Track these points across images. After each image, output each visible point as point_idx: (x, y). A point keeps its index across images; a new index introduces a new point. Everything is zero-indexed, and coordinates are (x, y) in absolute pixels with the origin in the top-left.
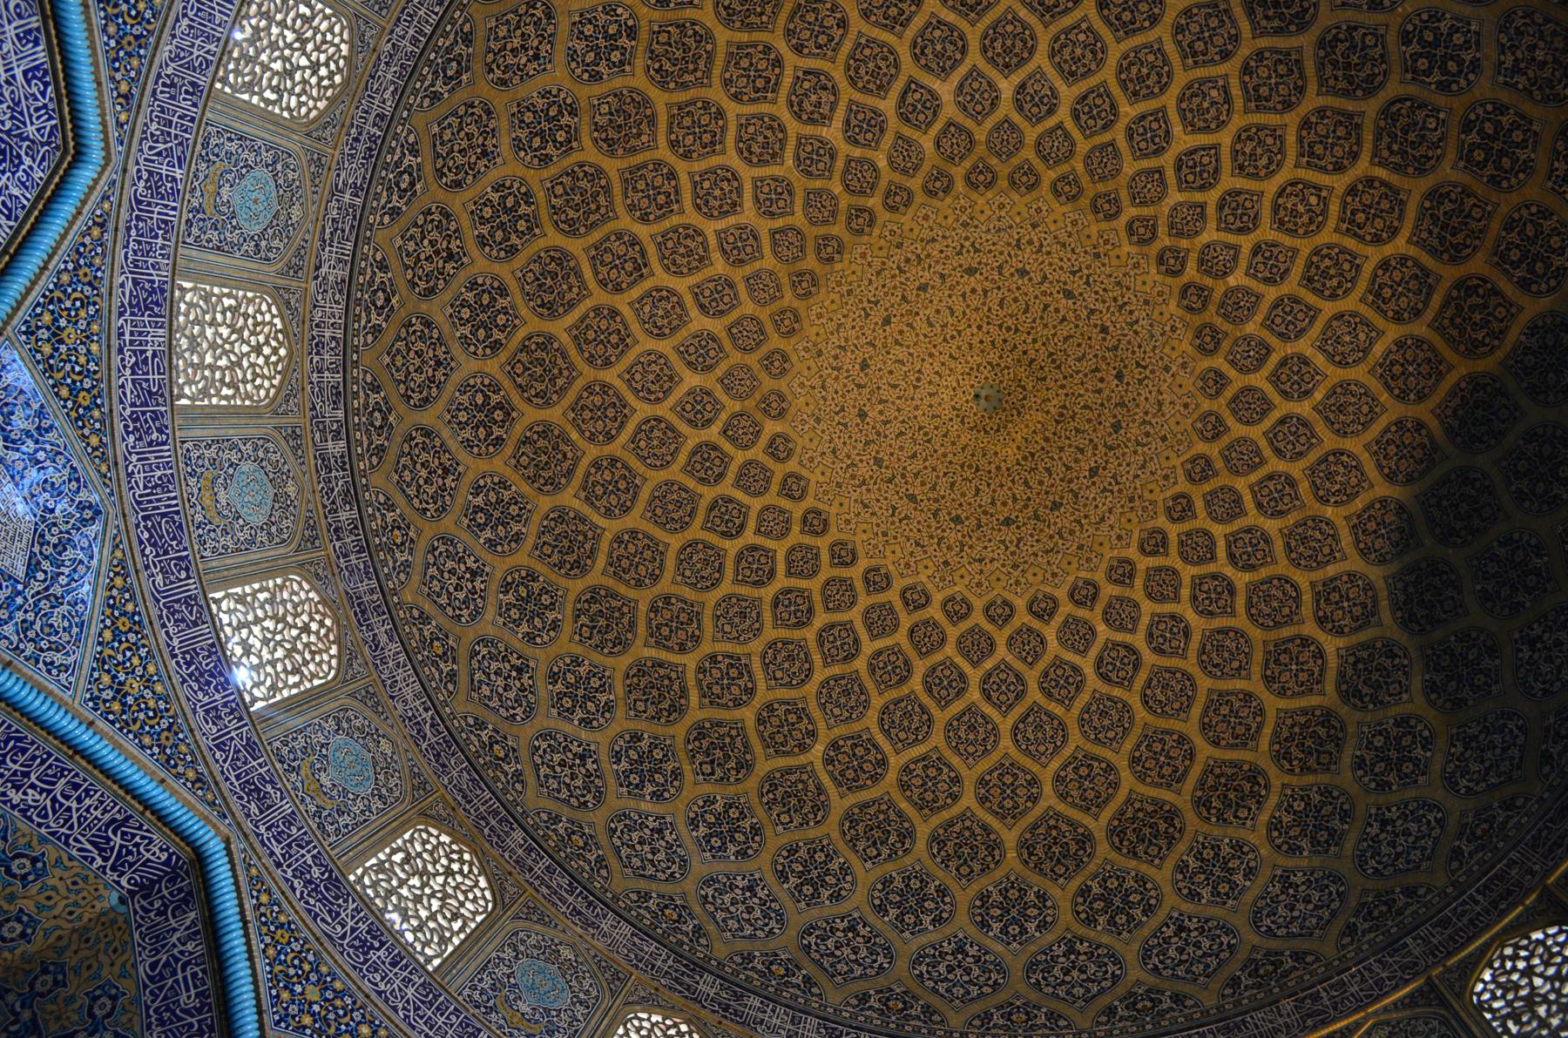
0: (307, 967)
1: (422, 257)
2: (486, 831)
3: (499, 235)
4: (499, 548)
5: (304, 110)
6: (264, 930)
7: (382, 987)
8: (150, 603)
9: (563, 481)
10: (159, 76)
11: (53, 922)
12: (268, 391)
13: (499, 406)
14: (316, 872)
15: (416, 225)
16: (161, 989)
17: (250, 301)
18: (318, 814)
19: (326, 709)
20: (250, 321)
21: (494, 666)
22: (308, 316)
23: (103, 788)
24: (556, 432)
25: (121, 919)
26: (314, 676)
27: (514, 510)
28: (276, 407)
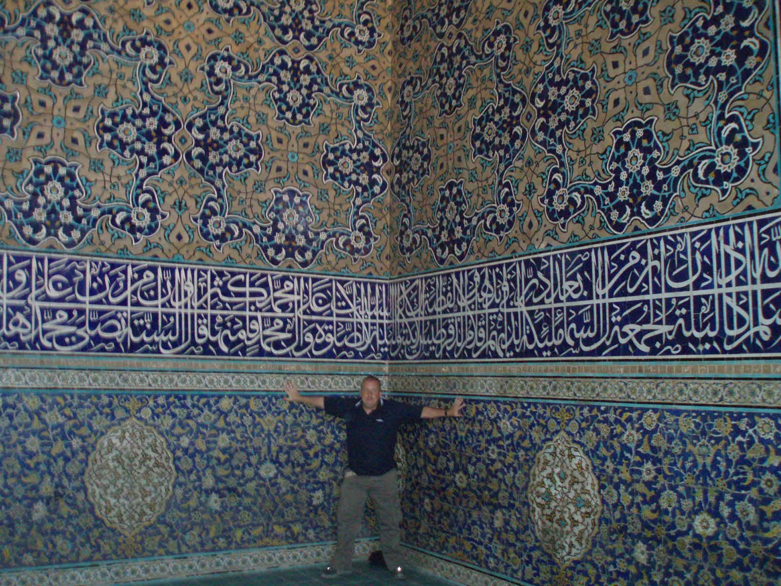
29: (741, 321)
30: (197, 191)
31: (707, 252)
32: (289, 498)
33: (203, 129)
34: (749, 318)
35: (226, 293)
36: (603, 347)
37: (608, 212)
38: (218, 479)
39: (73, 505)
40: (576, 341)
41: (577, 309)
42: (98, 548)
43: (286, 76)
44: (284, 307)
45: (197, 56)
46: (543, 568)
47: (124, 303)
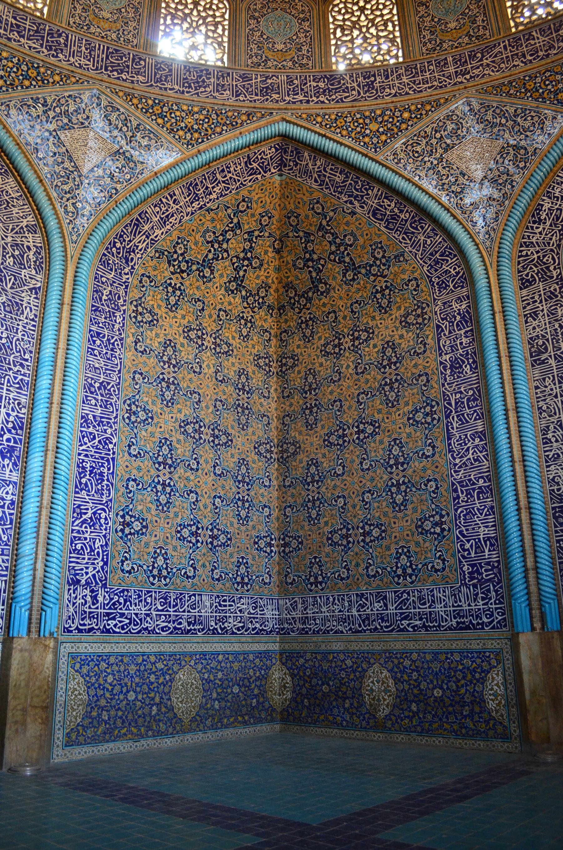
0: (361, 121)
6: (333, 129)
7: (393, 92)
11: (272, 205)
14: (321, 85)
16: (327, 184)
18: (294, 63)
19: (243, 20)
23: (229, 160)
25: (288, 180)
26: (223, 16)
29: (446, 620)
30: (210, 559)
31: (433, 596)
32: (244, 702)
33: (212, 530)
34: (449, 619)
35: (220, 605)
36: (394, 629)
37: (393, 578)
38: (218, 694)
39: (166, 707)
40: (382, 627)
41: (381, 614)
42: (174, 728)
43: (240, 503)
44: (240, 611)
45: (209, 497)
46: (371, 721)
47: (184, 611)
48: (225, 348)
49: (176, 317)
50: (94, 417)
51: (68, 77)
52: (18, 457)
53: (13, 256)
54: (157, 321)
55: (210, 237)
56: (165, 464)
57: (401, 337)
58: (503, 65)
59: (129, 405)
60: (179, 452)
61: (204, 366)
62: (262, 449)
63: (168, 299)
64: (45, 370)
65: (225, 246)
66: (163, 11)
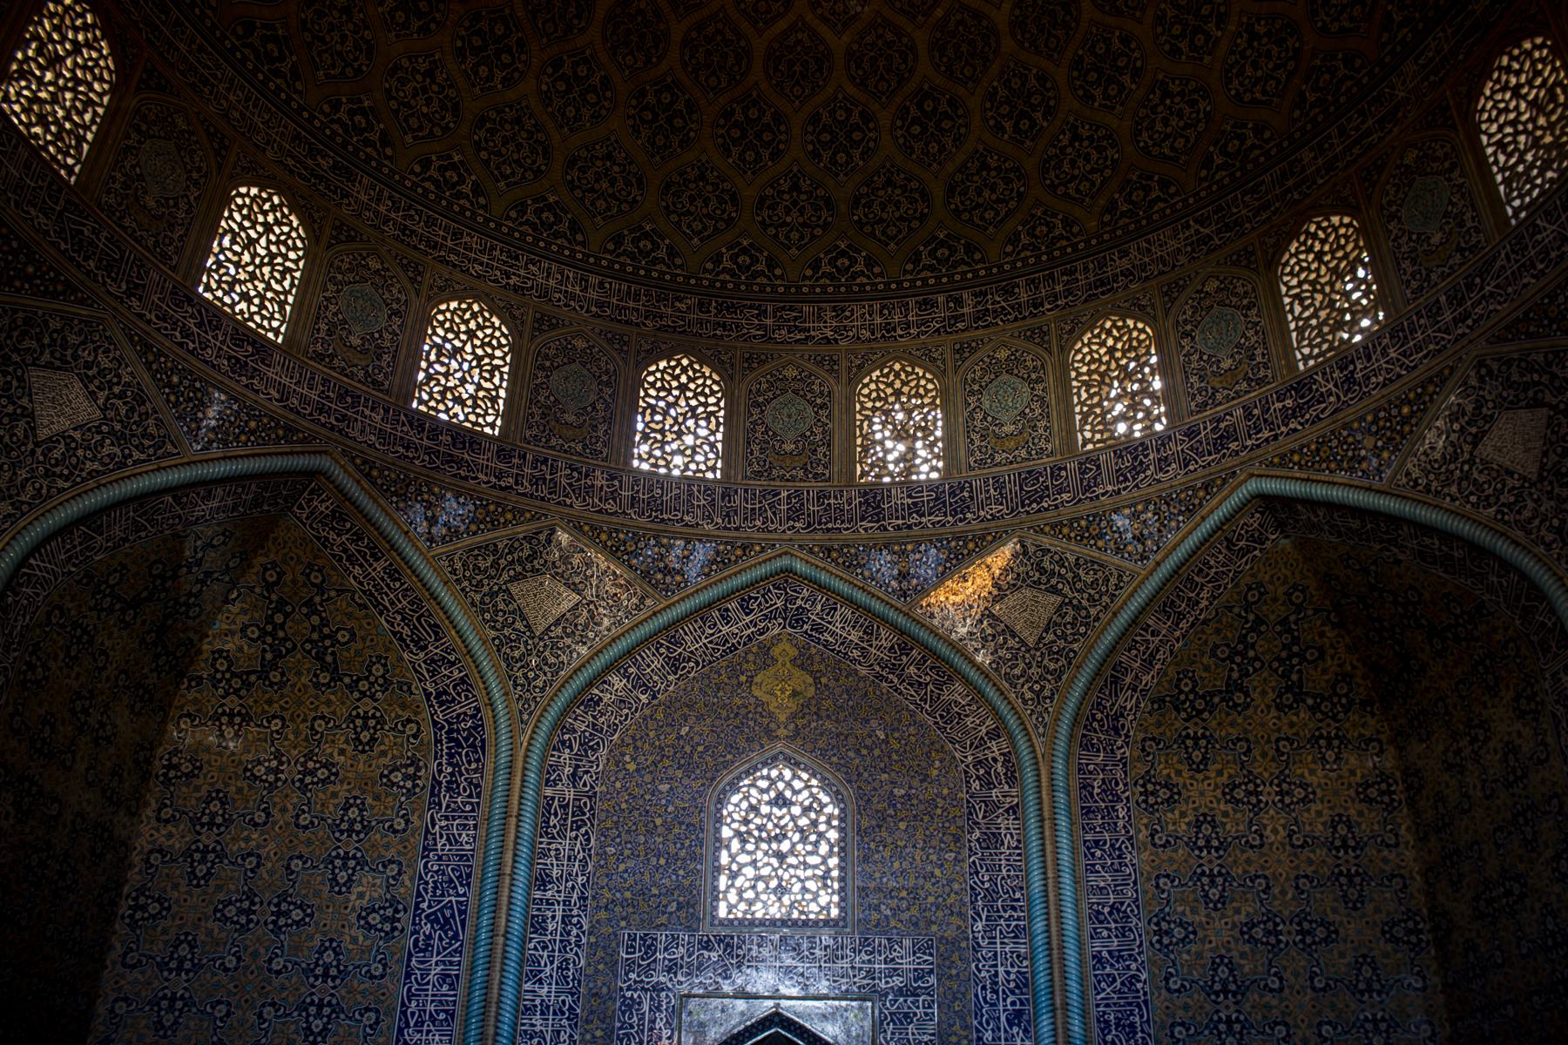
0: (1350, 440)
1: (801, 220)
2: (1296, 197)
3: (767, 137)
4: (1052, 103)
5: (715, 388)
8: (1081, 507)
9: (985, 23)
10: (725, 528)
12: (929, 381)
13: (920, 106)
14: (1289, 403)
15: (776, 236)
17: (863, 408)
20: (878, 404)
21: (1159, 127)
22: (867, 345)
24: (938, 35)
26: (1148, 353)
27: (1016, 83)
28: (941, 374)
43: (1369, 1026)
48: (1299, 793)
49: (1208, 778)
50: (1110, 952)
51: (983, 538)
52: (1028, 1022)
53: (978, 778)
54: (1179, 793)
55: (1223, 652)
56: (1225, 991)
57: (1519, 734)
58: (1510, 290)
59: (1157, 924)
60: (1246, 969)
61: (1267, 832)
62: (1399, 932)
63: (1190, 758)
64: (1038, 909)
65: (1251, 654)
66: (1075, 383)
